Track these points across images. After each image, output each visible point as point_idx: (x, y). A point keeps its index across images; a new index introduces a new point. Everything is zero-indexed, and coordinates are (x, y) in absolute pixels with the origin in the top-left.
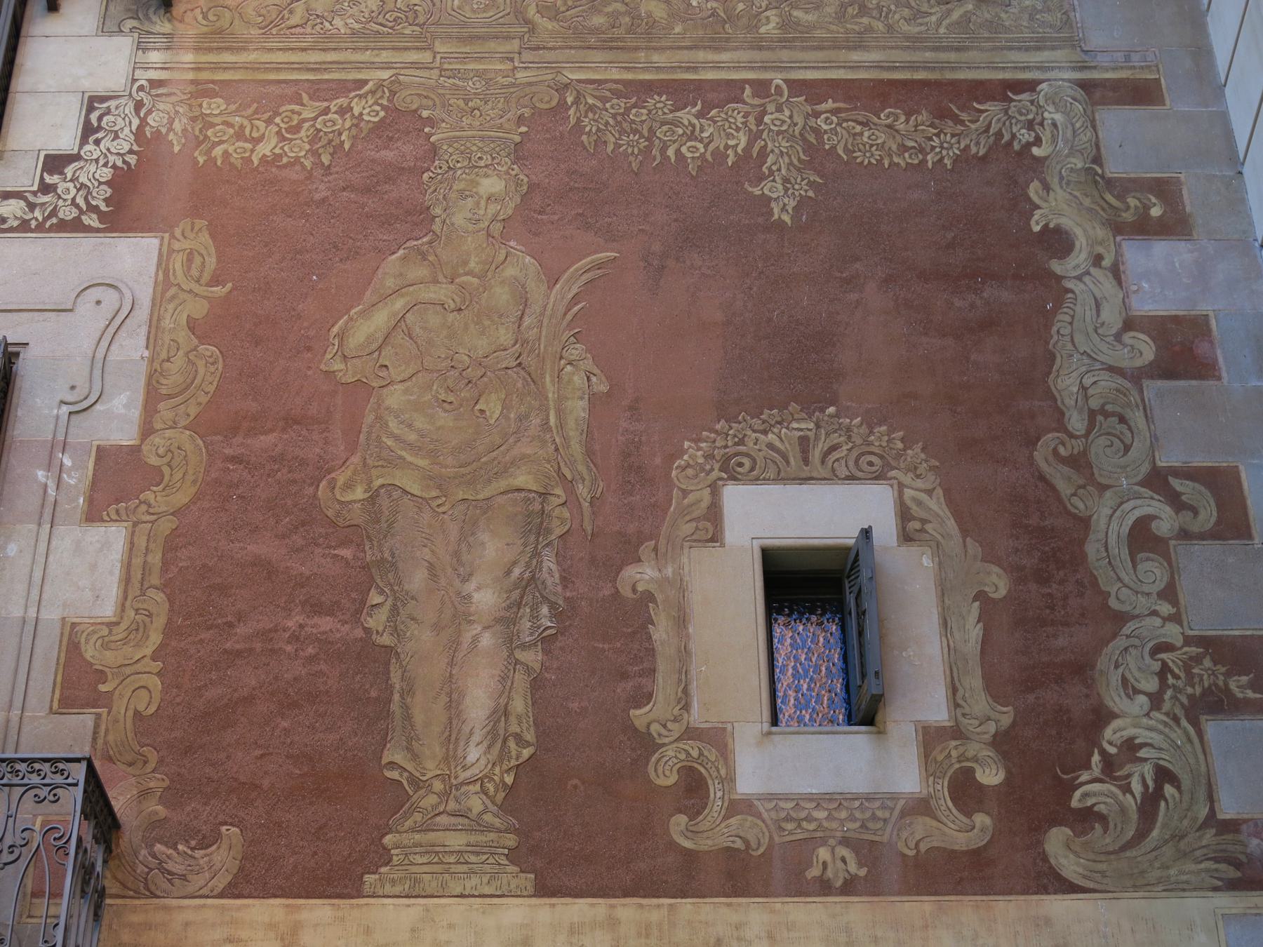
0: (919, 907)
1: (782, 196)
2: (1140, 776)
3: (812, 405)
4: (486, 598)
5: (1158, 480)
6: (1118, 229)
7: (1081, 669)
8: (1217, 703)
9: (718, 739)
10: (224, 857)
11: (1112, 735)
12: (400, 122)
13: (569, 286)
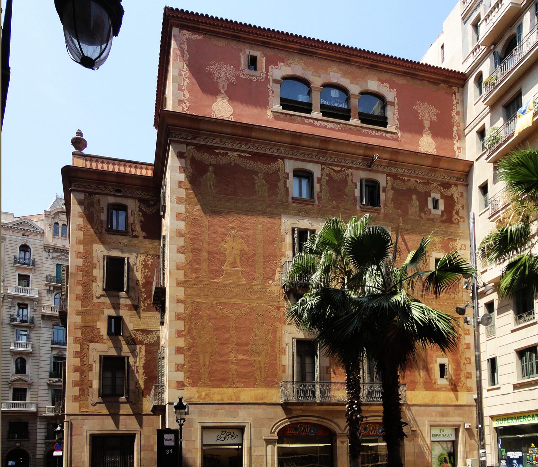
2: (463, 383)
5: (466, 359)
6: (465, 334)
7: (459, 374)
8: (468, 378)
9: (436, 379)
11: (461, 380)
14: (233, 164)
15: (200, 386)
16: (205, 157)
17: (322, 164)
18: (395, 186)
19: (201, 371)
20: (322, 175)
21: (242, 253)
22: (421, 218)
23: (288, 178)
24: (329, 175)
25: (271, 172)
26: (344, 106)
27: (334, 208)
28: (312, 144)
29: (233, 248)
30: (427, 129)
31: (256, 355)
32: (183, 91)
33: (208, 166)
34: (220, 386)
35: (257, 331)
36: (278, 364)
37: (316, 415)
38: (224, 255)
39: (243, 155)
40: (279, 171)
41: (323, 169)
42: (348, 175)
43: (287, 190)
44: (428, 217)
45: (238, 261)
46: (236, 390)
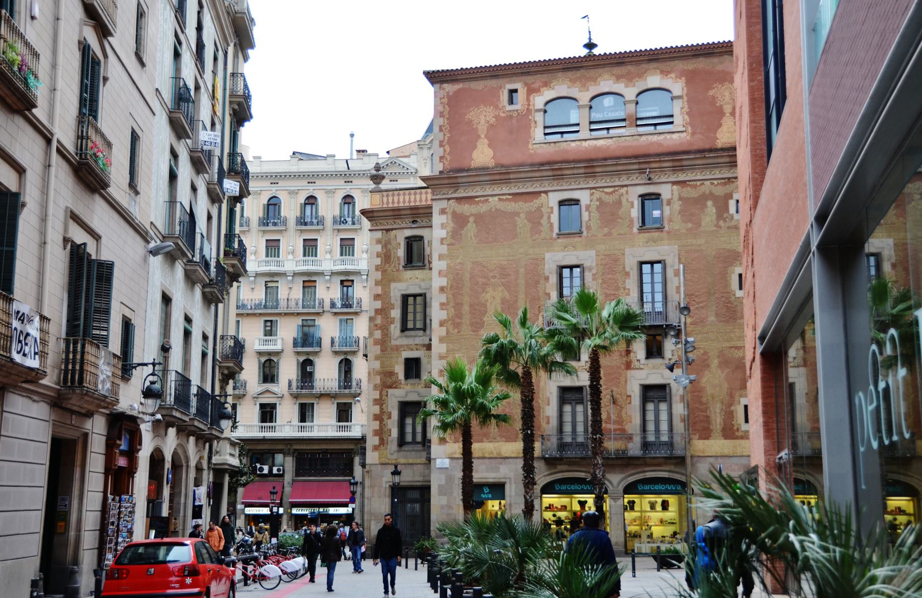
4: (718, 411)
10: (697, 436)
12: (705, 353)
16: (466, 209)
17: (591, 188)
18: (683, 195)
21: (503, 301)
23: (552, 212)
24: (599, 200)
27: (605, 235)
28: (575, 171)
30: (728, 115)
38: (486, 307)
39: (504, 197)
41: (592, 194)
44: (727, 225)
46: (496, 444)
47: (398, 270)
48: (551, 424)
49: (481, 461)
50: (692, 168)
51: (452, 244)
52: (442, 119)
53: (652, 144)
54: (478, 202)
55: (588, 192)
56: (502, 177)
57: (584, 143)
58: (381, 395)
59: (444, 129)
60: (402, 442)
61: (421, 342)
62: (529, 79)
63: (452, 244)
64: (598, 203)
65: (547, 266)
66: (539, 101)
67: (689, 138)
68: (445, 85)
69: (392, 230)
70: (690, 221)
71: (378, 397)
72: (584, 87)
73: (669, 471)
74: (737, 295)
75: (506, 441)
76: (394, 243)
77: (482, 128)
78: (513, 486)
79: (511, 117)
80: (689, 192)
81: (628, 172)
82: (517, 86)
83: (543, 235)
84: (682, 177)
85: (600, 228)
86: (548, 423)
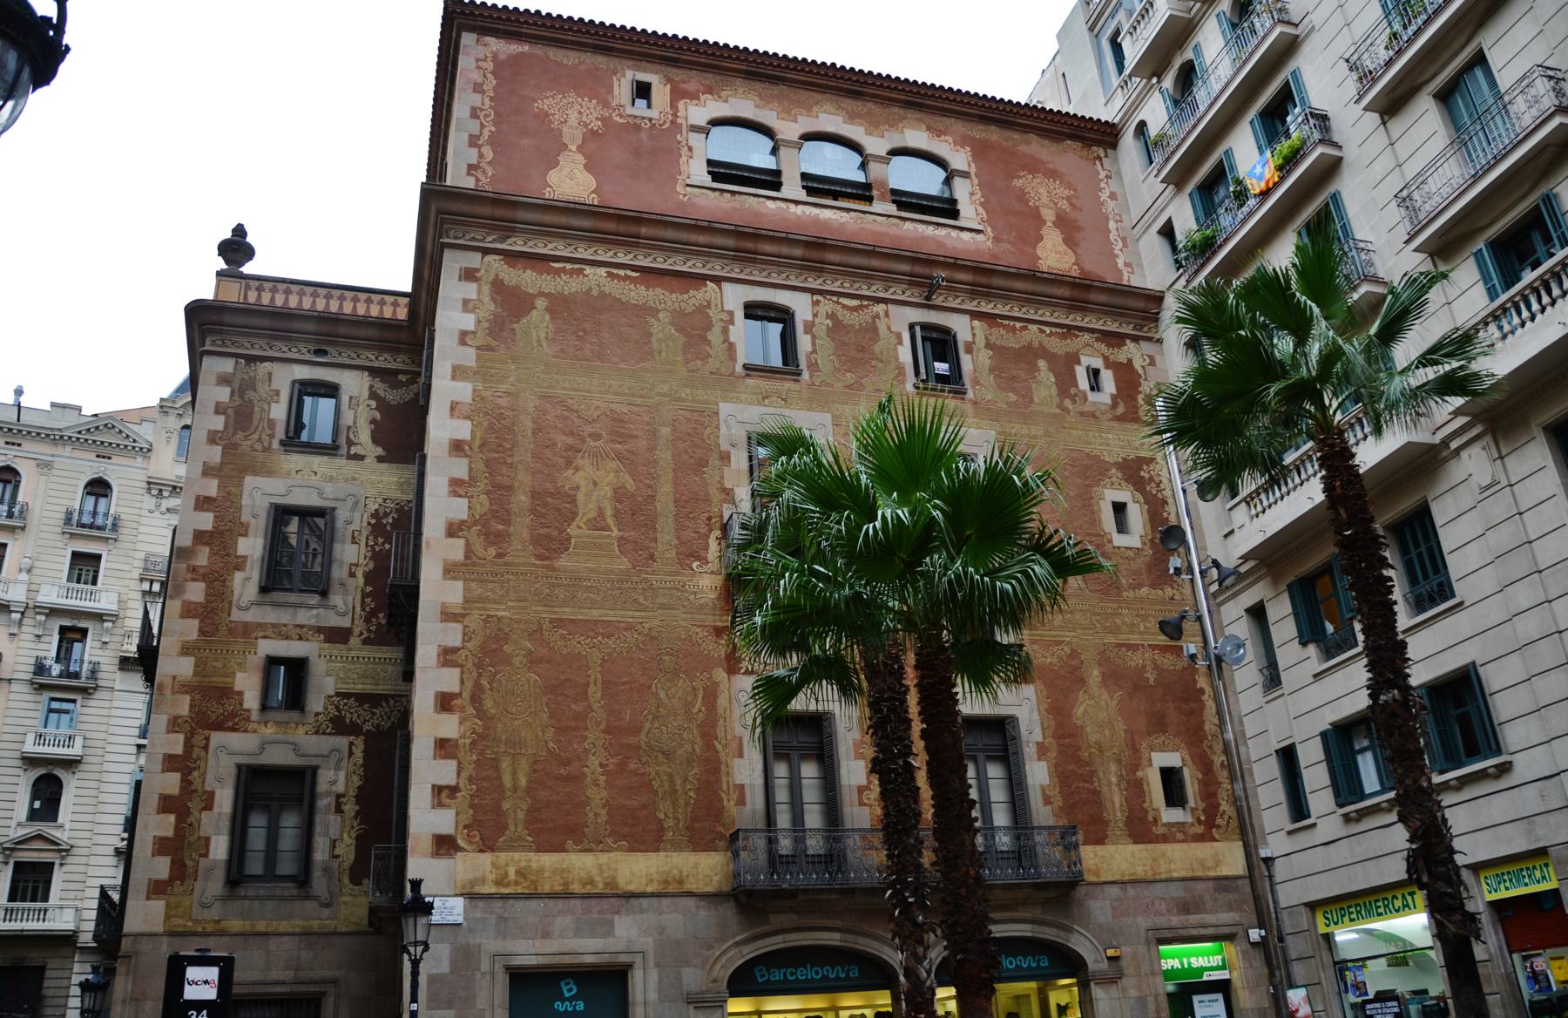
0: (1194, 845)
1: (1151, 676)
3: (1164, 732)
4: (1114, 780)
7: (1214, 795)
9: (1157, 810)
12: (1074, 654)
13: (1115, 702)
14: (595, 293)
15: (502, 850)
16: (527, 279)
17: (813, 291)
18: (993, 340)
19: (506, 806)
20: (815, 315)
21: (619, 494)
22: (1067, 410)
23: (732, 322)
25: (689, 310)
26: (859, 177)
27: (849, 387)
28: (785, 250)
29: (595, 483)
31: (661, 758)
32: (479, 147)
33: (534, 296)
34: (560, 848)
35: (662, 694)
36: (724, 779)
37: (839, 923)
38: (573, 501)
39: (622, 272)
40: (709, 306)
42: (877, 316)
43: (731, 347)
45: (609, 512)
46: (604, 858)
47: (267, 449)
48: (748, 806)
49: (560, 904)
50: (1005, 295)
51: (489, 348)
52: (478, 97)
53: (924, 238)
54: (558, 272)
55: (807, 297)
56: (623, 228)
57: (792, 207)
58: (188, 745)
59: (482, 115)
60: (236, 876)
61: (313, 622)
62: (678, 74)
63: (489, 348)
64: (829, 322)
65: (723, 429)
66: (699, 112)
67: (989, 243)
68: (488, 39)
69: (263, 359)
70: (1014, 390)
71: (179, 750)
72: (788, 114)
73: (1032, 921)
74: (1116, 543)
75: (631, 850)
76: (263, 389)
77: (572, 134)
78: (654, 975)
79: (638, 128)
80: (999, 335)
81: (888, 277)
82: (653, 78)
83: (712, 364)
84: (986, 307)
85: (837, 370)
86: (741, 802)
